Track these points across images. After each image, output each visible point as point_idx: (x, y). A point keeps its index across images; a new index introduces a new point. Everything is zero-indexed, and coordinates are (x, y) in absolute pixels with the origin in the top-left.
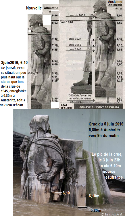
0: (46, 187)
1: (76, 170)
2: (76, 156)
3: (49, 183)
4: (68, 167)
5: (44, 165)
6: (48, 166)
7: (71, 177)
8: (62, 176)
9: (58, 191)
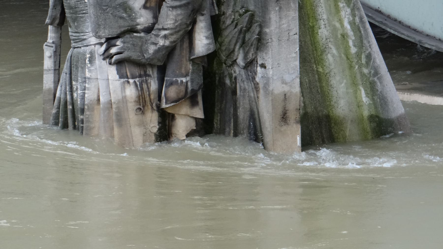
0: (140, 89)
1: (257, 18)
3: (154, 73)
4: (223, 8)
6: (145, 7)
7: (237, 47)
9: (188, 103)
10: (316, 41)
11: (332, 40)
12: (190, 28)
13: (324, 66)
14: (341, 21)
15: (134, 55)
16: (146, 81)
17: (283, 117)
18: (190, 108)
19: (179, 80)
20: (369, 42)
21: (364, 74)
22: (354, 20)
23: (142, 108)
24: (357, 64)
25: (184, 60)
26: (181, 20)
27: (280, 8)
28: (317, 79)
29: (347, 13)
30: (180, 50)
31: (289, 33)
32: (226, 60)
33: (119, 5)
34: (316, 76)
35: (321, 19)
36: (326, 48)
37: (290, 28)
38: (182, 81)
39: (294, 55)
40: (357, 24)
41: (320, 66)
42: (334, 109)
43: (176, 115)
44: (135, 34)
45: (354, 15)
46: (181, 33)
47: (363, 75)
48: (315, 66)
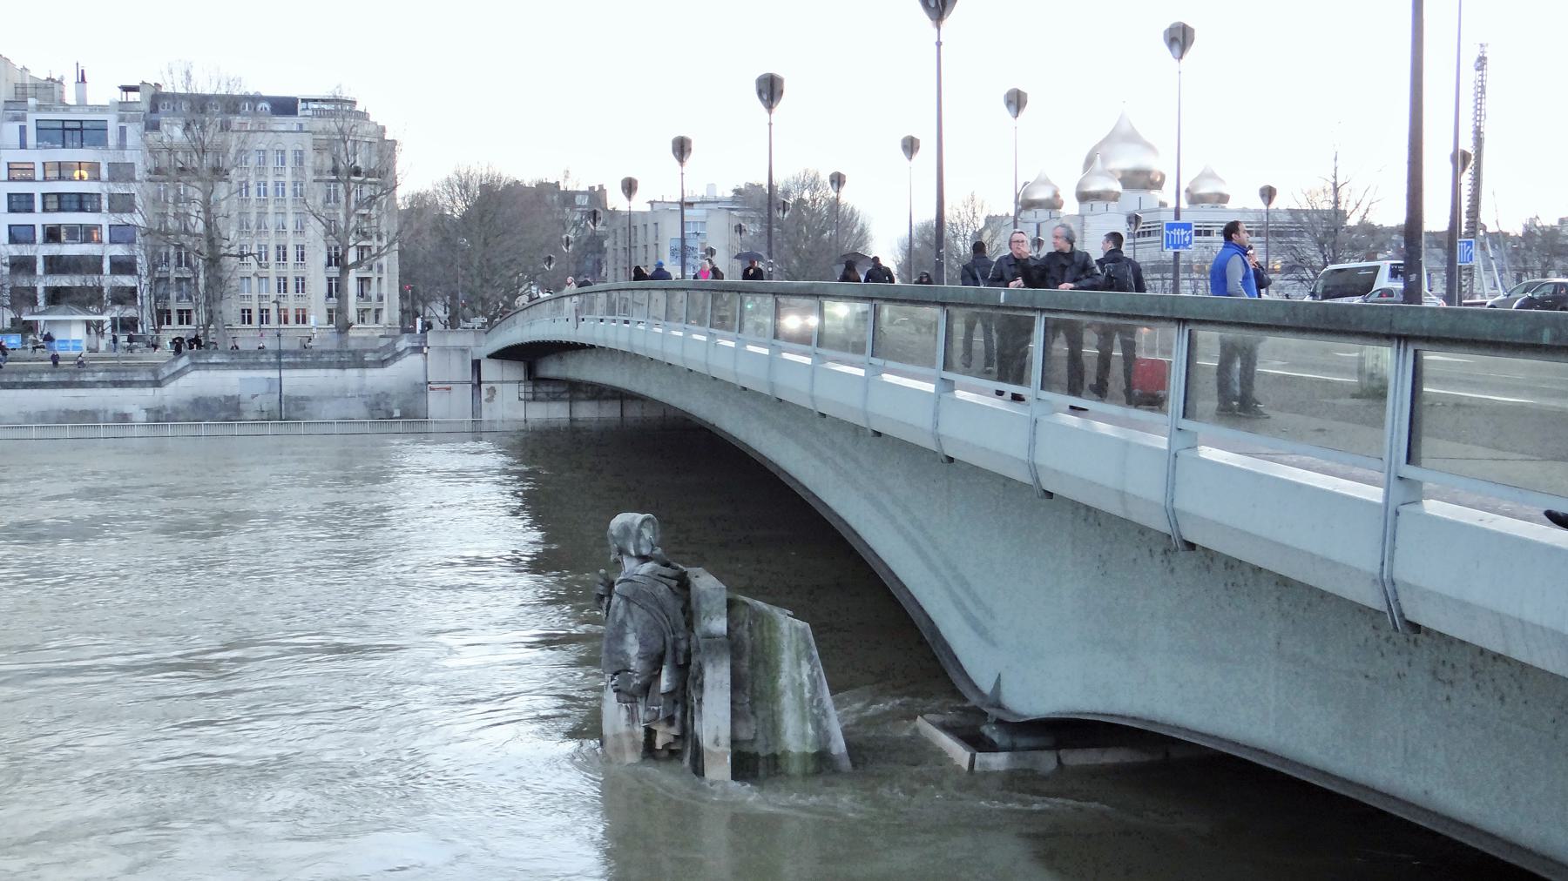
2: (703, 629)
5: (628, 651)
8: (665, 683)
12: (657, 673)
14: (800, 675)
27: (714, 666)
45: (813, 671)
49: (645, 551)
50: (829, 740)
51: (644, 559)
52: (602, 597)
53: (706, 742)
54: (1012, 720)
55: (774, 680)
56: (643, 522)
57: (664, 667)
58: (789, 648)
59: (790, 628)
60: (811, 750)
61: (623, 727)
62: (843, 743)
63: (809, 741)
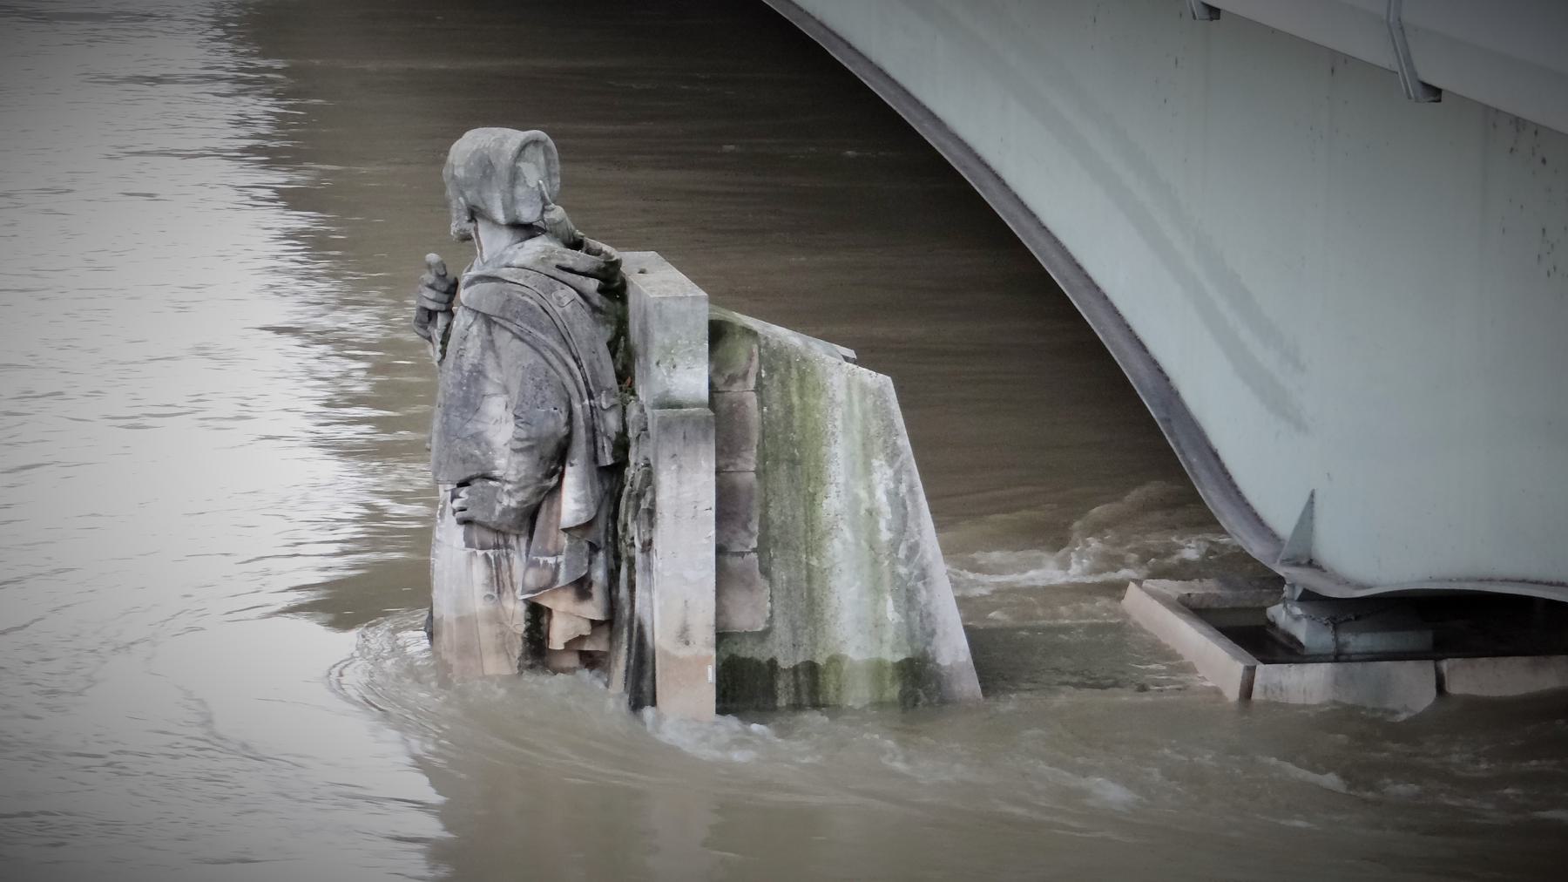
2: (658, 390)
5: (489, 435)
10: (813, 518)
11: (847, 517)
13: (824, 557)
15: (479, 516)
16: (508, 554)
17: (680, 636)
18: (574, 602)
19: (542, 560)
20: (919, 525)
21: (899, 576)
22: (897, 487)
23: (496, 596)
24: (886, 558)
25: (553, 531)
26: (525, 470)
27: (680, 467)
28: (804, 577)
29: (885, 476)
30: (547, 513)
31: (695, 507)
32: (624, 537)
33: (472, 436)
34: (804, 572)
35: (831, 484)
36: (832, 529)
37: (698, 500)
38: (545, 562)
39: (705, 541)
40: (901, 495)
41: (814, 558)
42: (826, 626)
43: (553, 611)
44: (491, 483)
45: (898, 481)
46: (530, 490)
47: (896, 576)
48: (804, 556)
49: (528, 214)
50: (933, 633)
51: (526, 230)
52: (431, 315)
53: (661, 638)
54: (1336, 592)
55: (811, 500)
56: (524, 147)
57: (568, 470)
58: (846, 431)
59: (849, 387)
60: (892, 656)
61: (478, 603)
62: (963, 643)
63: (889, 635)
